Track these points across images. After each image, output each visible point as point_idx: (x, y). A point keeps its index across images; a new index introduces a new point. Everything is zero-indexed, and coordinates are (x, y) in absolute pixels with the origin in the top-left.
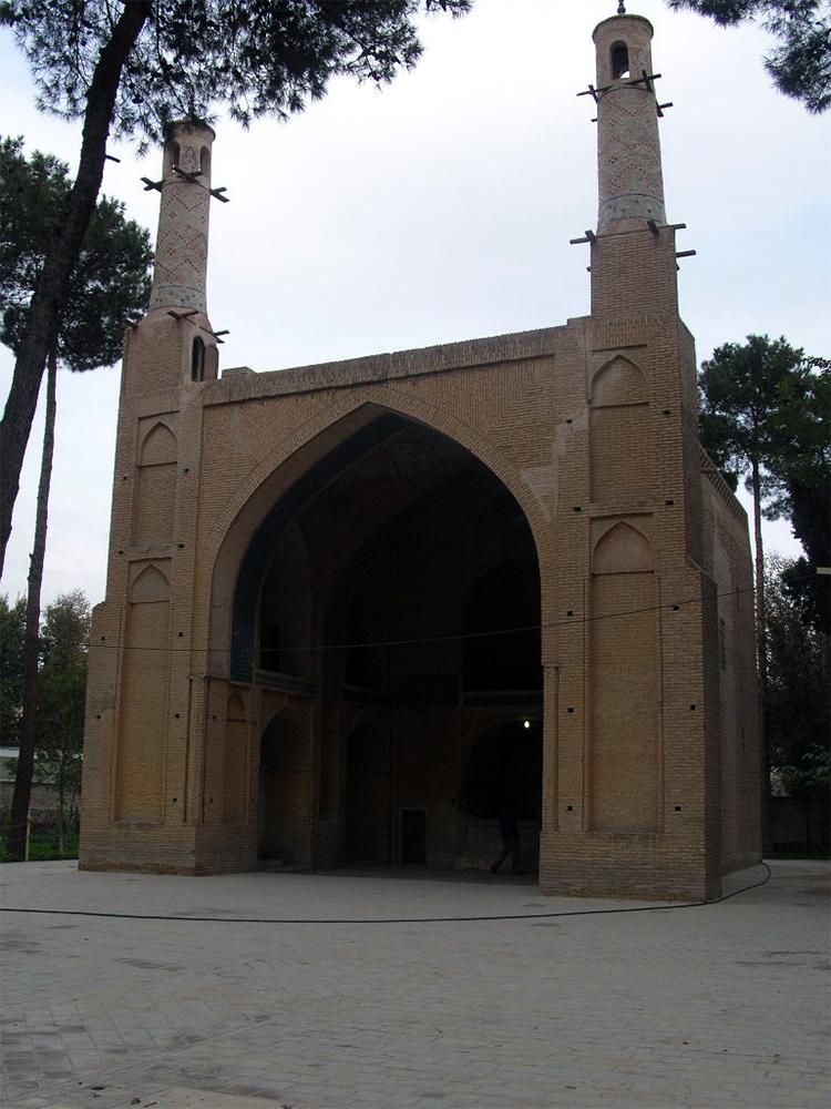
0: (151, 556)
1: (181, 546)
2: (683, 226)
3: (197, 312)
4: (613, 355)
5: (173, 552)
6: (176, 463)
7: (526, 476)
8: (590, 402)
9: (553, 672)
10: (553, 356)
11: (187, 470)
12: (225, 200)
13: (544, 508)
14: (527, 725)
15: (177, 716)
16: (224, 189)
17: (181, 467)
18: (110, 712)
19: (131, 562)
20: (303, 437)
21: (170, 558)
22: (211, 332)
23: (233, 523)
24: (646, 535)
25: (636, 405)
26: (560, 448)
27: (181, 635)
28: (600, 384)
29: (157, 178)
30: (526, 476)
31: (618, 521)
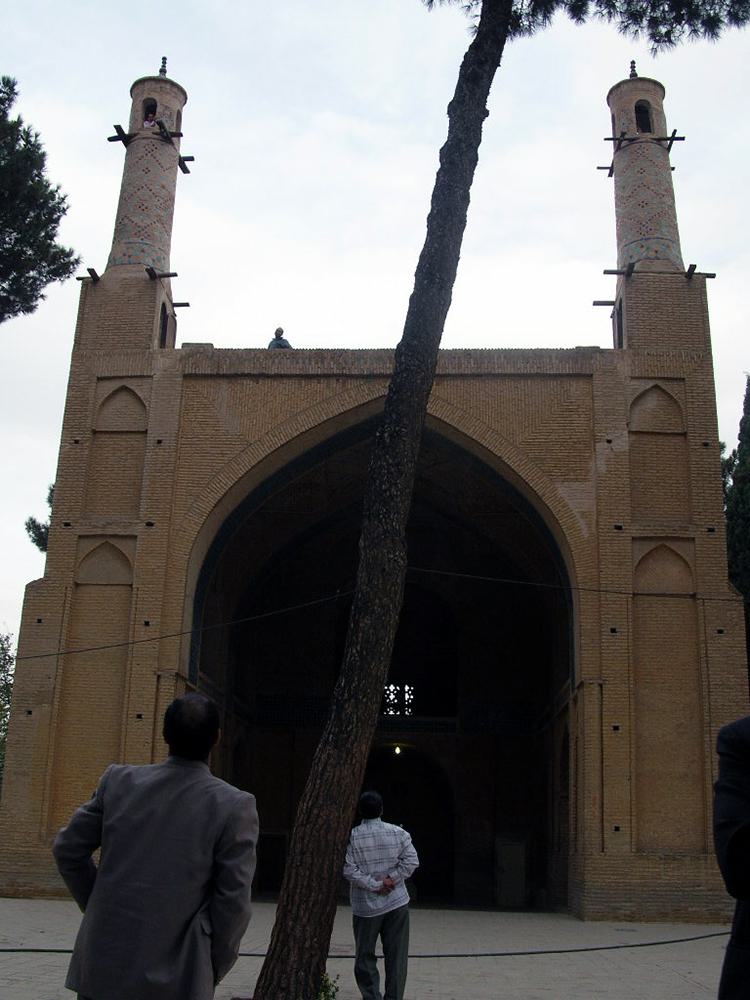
0: (109, 531)
1: (150, 524)
2: (713, 276)
4: (651, 384)
5: (139, 529)
6: (146, 432)
7: (562, 490)
9: (597, 688)
11: (159, 442)
13: (582, 523)
14: (398, 751)
15: (139, 716)
17: (152, 437)
18: (46, 707)
19: (80, 537)
20: (306, 422)
21: (136, 537)
22: (171, 301)
24: (687, 559)
25: (671, 434)
26: (600, 464)
27: (147, 624)
28: (637, 410)
30: (562, 490)
31: (660, 543)
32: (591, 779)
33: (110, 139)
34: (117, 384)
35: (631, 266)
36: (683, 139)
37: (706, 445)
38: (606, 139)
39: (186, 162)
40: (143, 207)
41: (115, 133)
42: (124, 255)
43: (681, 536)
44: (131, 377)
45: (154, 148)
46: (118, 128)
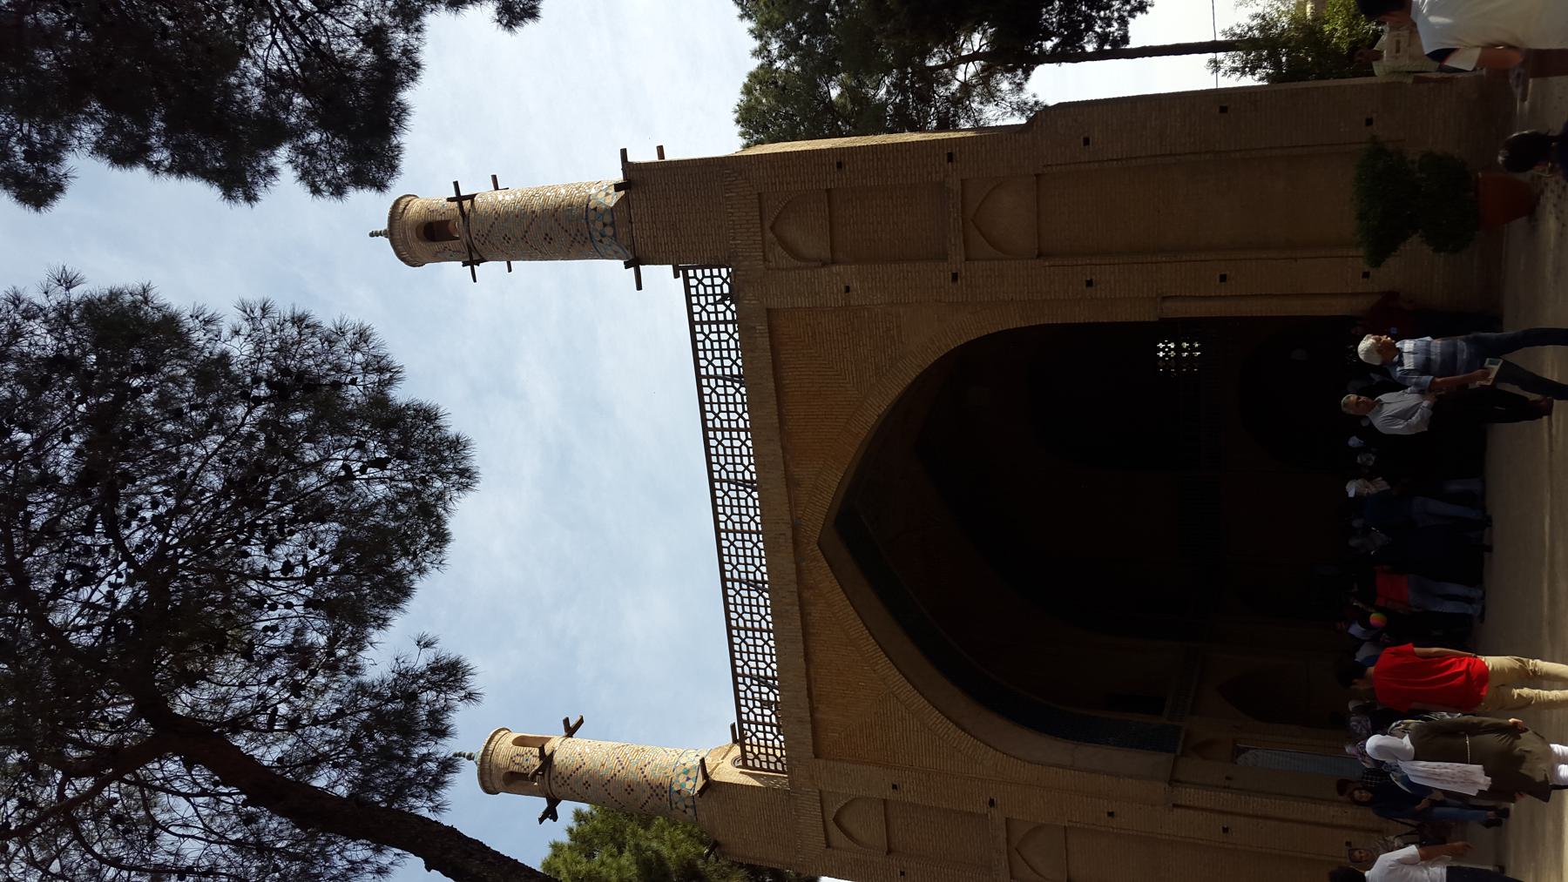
1: (992, 803)
2: (624, 152)
3: (702, 761)
4: (770, 235)
8: (824, 264)
10: (769, 310)
11: (894, 787)
12: (581, 722)
15: (1225, 830)
16: (566, 721)
17: (889, 794)
21: (1007, 818)
23: (963, 730)
29: (542, 804)
32: (1296, 308)
33: (555, 818)
34: (833, 828)
37: (840, 165)
38: (475, 281)
39: (571, 725)
40: (629, 789)
42: (685, 811)
43: (960, 198)
44: (822, 812)
45: (560, 777)
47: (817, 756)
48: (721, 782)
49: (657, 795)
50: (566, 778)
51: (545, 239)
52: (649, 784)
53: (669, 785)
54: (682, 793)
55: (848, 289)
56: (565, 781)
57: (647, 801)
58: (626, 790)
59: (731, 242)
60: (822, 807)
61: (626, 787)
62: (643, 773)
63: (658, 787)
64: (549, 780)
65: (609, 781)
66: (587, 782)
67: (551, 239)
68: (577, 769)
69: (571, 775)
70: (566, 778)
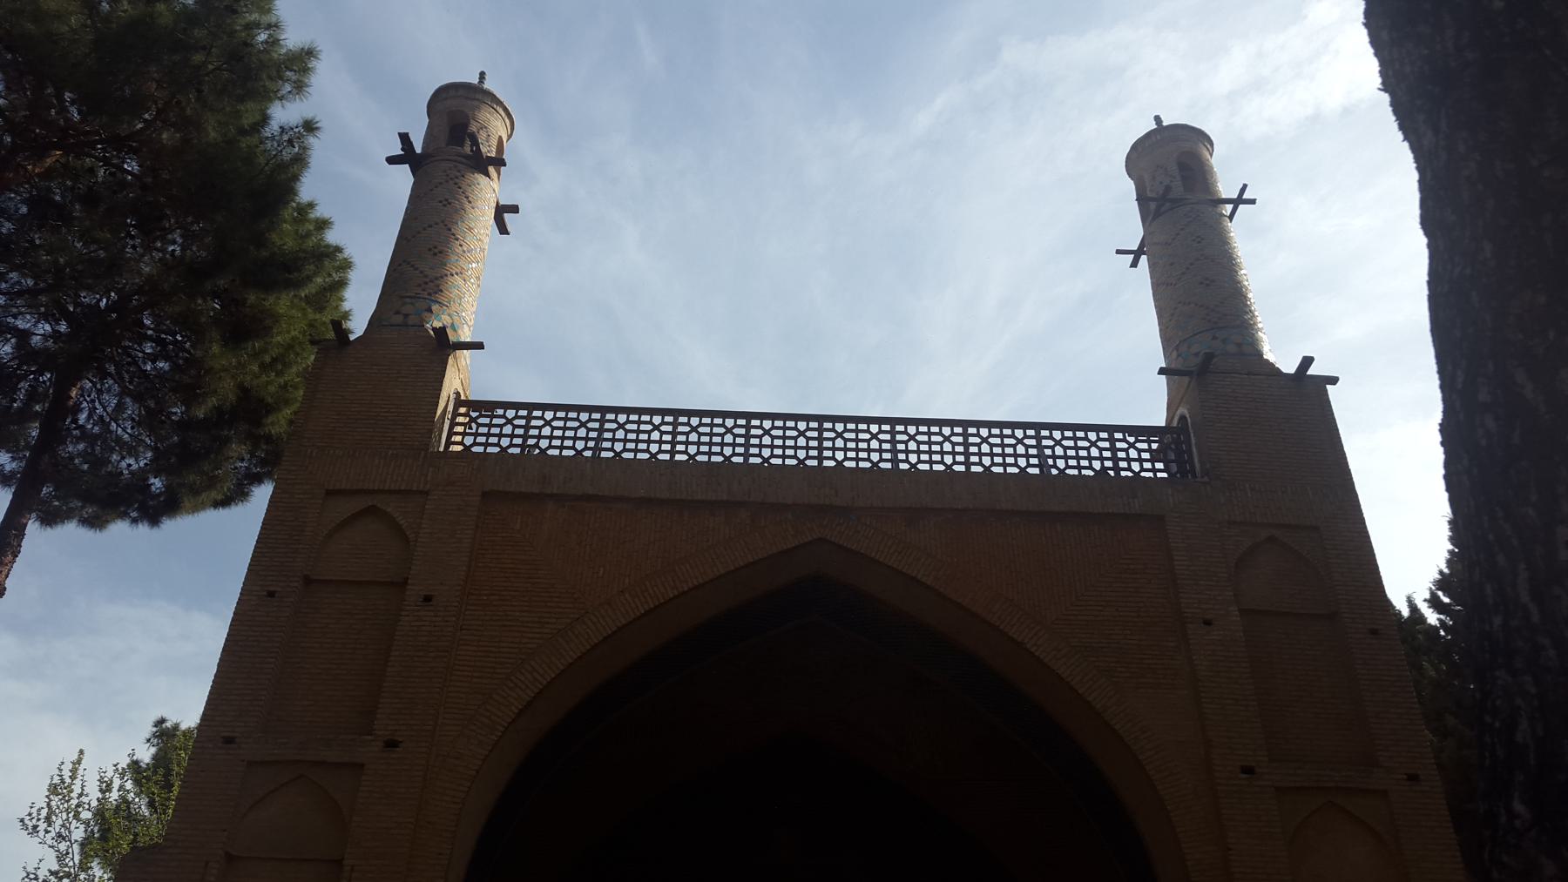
1: (391, 744)
6: (405, 582)
11: (428, 599)
16: (514, 209)
21: (362, 766)
33: (392, 160)
35: (1209, 357)
36: (1253, 202)
39: (505, 214)
40: (436, 251)
41: (397, 150)
42: (398, 313)
44: (390, 492)
46: (405, 138)
47: (485, 495)
48: (446, 368)
49: (426, 283)
50: (457, 181)
51: (1207, 279)
52: (442, 277)
53: (439, 300)
54: (426, 314)
55: (1208, 623)
56: (451, 179)
57: (417, 269)
58: (435, 248)
59: (1247, 486)
60: (399, 492)
61: (440, 248)
62: (457, 274)
63: (438, 286)
64: (455, 161)
65: (450, 230)
66: (450, 204)
67: (1208, 285)
68: (467, 197)
69: (460, 188)
70: (457, 181)
